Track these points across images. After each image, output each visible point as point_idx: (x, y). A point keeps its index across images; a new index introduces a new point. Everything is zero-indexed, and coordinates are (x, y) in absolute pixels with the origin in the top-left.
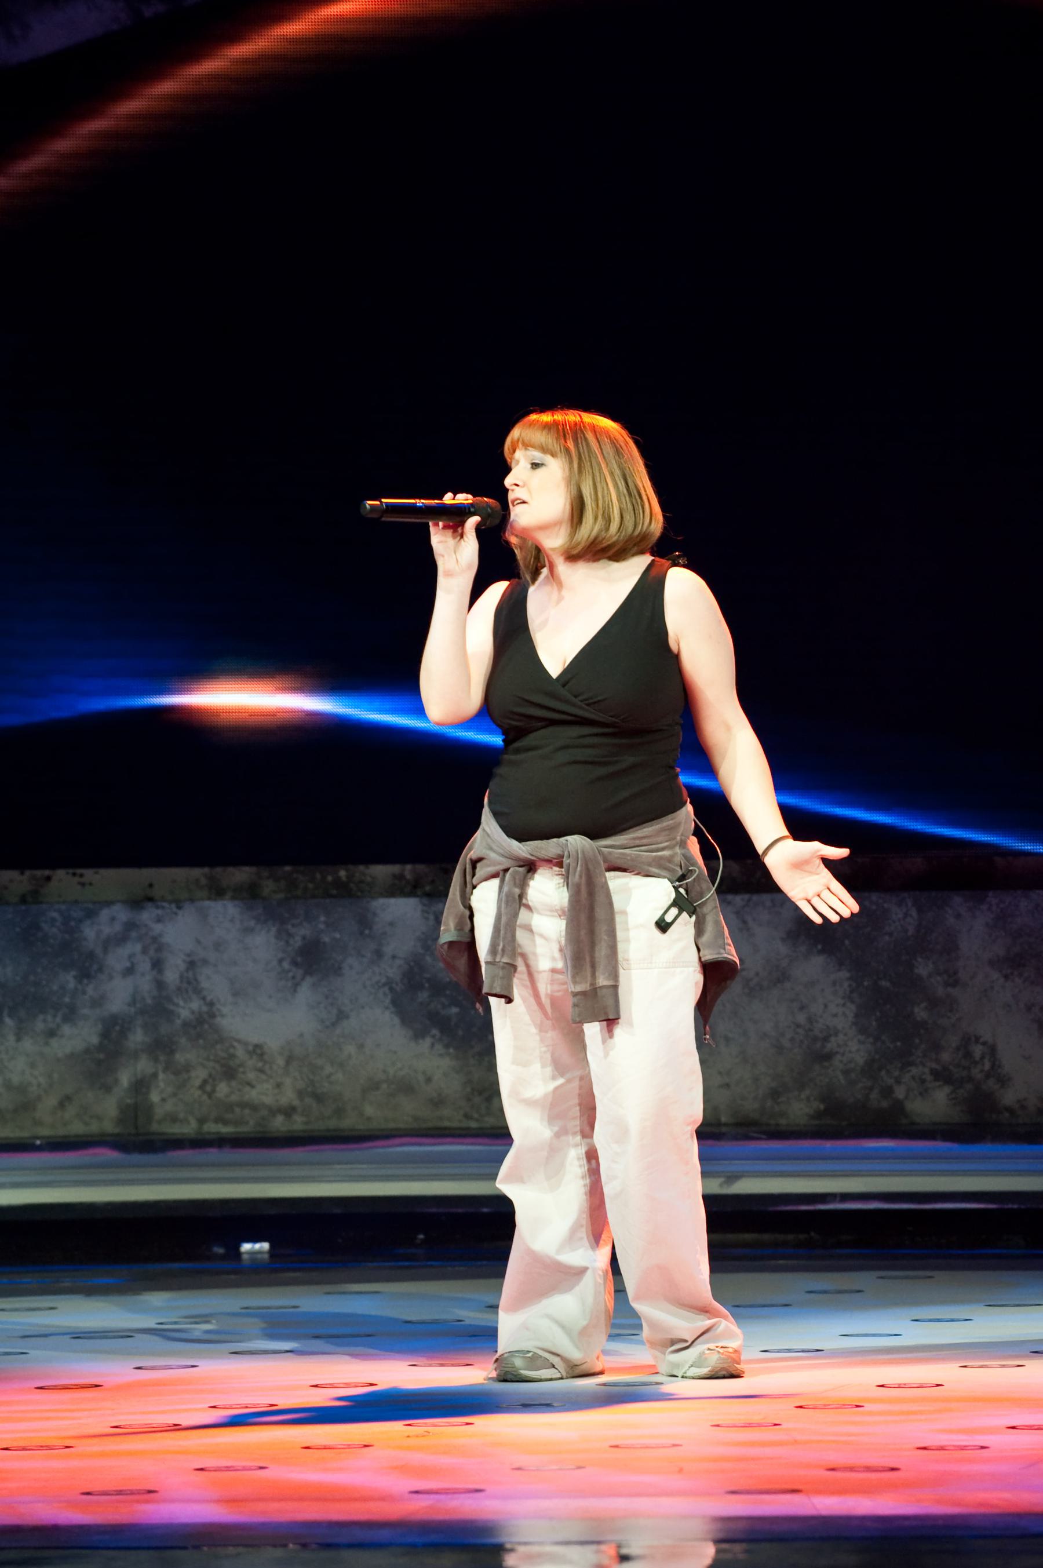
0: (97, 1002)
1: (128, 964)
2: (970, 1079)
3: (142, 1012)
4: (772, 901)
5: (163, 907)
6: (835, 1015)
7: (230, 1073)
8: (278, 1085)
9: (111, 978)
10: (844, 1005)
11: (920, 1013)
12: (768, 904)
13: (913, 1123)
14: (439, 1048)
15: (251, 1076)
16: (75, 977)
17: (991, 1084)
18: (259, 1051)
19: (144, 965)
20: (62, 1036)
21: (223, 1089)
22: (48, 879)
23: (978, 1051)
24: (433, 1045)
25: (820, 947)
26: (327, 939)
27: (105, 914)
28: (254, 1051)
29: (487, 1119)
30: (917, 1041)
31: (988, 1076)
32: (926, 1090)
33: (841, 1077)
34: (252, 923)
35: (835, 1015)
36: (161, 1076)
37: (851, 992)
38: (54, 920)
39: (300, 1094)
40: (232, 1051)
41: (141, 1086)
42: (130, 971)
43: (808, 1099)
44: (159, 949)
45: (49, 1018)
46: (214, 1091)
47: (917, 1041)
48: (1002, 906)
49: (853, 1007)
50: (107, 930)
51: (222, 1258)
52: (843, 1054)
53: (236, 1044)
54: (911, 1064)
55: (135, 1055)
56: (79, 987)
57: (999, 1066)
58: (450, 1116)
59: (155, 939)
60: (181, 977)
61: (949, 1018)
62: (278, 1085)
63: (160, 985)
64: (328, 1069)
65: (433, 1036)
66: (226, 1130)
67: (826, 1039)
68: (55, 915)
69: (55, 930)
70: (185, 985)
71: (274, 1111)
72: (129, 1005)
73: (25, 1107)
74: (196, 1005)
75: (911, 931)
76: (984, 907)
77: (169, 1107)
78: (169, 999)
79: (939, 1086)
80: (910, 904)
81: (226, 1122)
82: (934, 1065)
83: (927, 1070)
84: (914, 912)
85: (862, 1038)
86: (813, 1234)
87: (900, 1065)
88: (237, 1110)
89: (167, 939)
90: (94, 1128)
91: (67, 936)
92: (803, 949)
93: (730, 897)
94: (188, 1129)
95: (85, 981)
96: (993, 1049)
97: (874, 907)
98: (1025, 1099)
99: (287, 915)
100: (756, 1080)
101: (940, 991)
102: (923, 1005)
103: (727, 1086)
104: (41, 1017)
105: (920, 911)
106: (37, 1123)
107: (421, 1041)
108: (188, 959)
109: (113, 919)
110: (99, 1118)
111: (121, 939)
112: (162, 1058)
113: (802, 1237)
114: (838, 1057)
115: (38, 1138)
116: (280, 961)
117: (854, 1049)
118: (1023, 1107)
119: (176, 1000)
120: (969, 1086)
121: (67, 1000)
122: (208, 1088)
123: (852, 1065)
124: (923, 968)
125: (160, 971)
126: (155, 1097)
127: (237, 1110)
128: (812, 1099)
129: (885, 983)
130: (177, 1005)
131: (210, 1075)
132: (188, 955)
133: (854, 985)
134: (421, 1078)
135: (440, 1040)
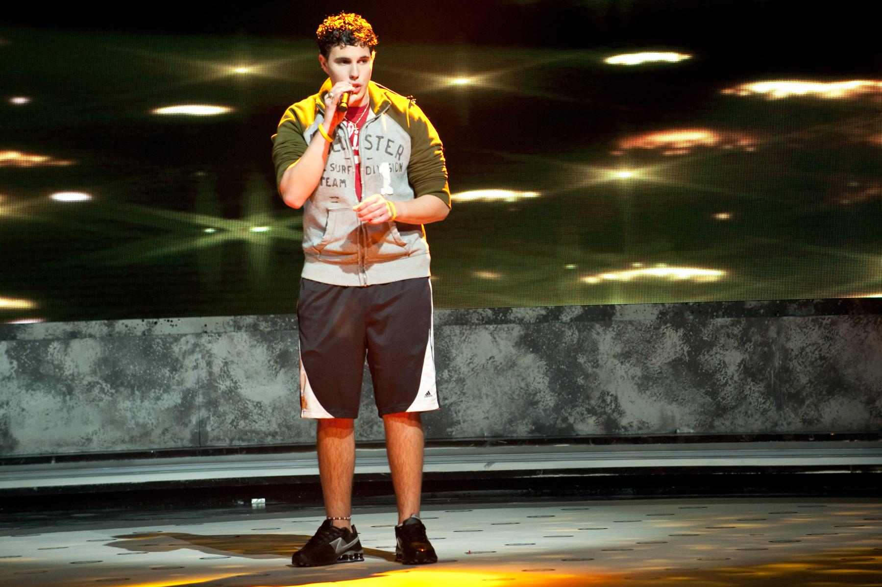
0: (180, 383)
1: (195, 364)
2: (605, 413)
3: (202, 387)
4: (508, 328)
5: (212, 336)
6: (539, 383)
7: (245, 416)
8: (269, 422)
9: (187, 371)
10: (543, 378)
11: (580, 381)
12: (506, 329)
13: (577, 435)
15: (256, 417)
16: (169, 371)
17: (616, 415)
18: (259, 405)
19: (203, 364)
20: (163, 400)
21: (242, 424)
22: (156, 323)
23: (609, 399)
25: (531, 349)
26: (292, 350)
27: (183, 339)
28: (257, 405)
29: (370, 436)
31: (614, 411)
32: (584, 418)
33: (543, 413)
34: (255, 343)
35: (539, 383)
36: (212, 418)
37: (547, 371)
38: (158, 343)
39: (279, 425)
40: (246, 405)
41: (202, 423)
42: (196, 367)
43: (527, 424)
44: (210, 357)
45: (157, 391)
46: (237, 425)
47: (579, 395)
48: (619, 328)
49: (548, 379)
50: (184, 348)
51: (244, 505)
52: (543, 402)
53: (248, 402)
54: (577, 406)
55: (199, 408)
56: (171, 375)
57: (619, 406)
59: (208, 352)
60: (221, 370)
62: (269, 422)
63: (211, 373)
64: (293, 413)
66: (244, 444)
67: (535, 394)
68: (160, 341)
70: (223, 373)
71: (267, 435)
72: (196, 384)
73: (146, 434)
75: (575, 340)
76: (611, 329)
77: (215, 433)
78: (215, 381)
79: (590, 417)
80: (575, 328)
81: (243, 440)
82: (587, 406)
83: (584, 409)
84: (577, 333)
85: (553, 394)
86: (530, 490)
88: (249, 434)
89: (213, 351)
90: (179, 444)
91: (165, 351)
92: (523, 351)
93: (487, 326)
94: (225, 444)
95: (174, 372)
96: (616, 398)
97: (557, 330)
98: (632, 422)
99: (272, 338)
100: (501, 415)
101: (590, 370)
102: (581, 377)
103: (487, 418)
104: (153, 390)
105: (579, 331)
106: (152, 442)
108: (224, 361)
109: (187, 342)
110: (182, 439)
111: (192, 352)
112: (212, 409)
113: (524, 491)
114: (541, 403)
115: (152, 449)
116: (269, 361)
117: (549, 399)
118: (631, 426)
119: (218, 381)
120: (605, 416)
121: (165, 382)
122: (235, 424)
123: (548, 407)
124: (581, 360)
125: (211, 367)
126: (209, 429)
127: (249, 434)
128: (528, 424)
130: (219, 384)
131: (235, 418)
132: (224, 359)
133: (548, 368)
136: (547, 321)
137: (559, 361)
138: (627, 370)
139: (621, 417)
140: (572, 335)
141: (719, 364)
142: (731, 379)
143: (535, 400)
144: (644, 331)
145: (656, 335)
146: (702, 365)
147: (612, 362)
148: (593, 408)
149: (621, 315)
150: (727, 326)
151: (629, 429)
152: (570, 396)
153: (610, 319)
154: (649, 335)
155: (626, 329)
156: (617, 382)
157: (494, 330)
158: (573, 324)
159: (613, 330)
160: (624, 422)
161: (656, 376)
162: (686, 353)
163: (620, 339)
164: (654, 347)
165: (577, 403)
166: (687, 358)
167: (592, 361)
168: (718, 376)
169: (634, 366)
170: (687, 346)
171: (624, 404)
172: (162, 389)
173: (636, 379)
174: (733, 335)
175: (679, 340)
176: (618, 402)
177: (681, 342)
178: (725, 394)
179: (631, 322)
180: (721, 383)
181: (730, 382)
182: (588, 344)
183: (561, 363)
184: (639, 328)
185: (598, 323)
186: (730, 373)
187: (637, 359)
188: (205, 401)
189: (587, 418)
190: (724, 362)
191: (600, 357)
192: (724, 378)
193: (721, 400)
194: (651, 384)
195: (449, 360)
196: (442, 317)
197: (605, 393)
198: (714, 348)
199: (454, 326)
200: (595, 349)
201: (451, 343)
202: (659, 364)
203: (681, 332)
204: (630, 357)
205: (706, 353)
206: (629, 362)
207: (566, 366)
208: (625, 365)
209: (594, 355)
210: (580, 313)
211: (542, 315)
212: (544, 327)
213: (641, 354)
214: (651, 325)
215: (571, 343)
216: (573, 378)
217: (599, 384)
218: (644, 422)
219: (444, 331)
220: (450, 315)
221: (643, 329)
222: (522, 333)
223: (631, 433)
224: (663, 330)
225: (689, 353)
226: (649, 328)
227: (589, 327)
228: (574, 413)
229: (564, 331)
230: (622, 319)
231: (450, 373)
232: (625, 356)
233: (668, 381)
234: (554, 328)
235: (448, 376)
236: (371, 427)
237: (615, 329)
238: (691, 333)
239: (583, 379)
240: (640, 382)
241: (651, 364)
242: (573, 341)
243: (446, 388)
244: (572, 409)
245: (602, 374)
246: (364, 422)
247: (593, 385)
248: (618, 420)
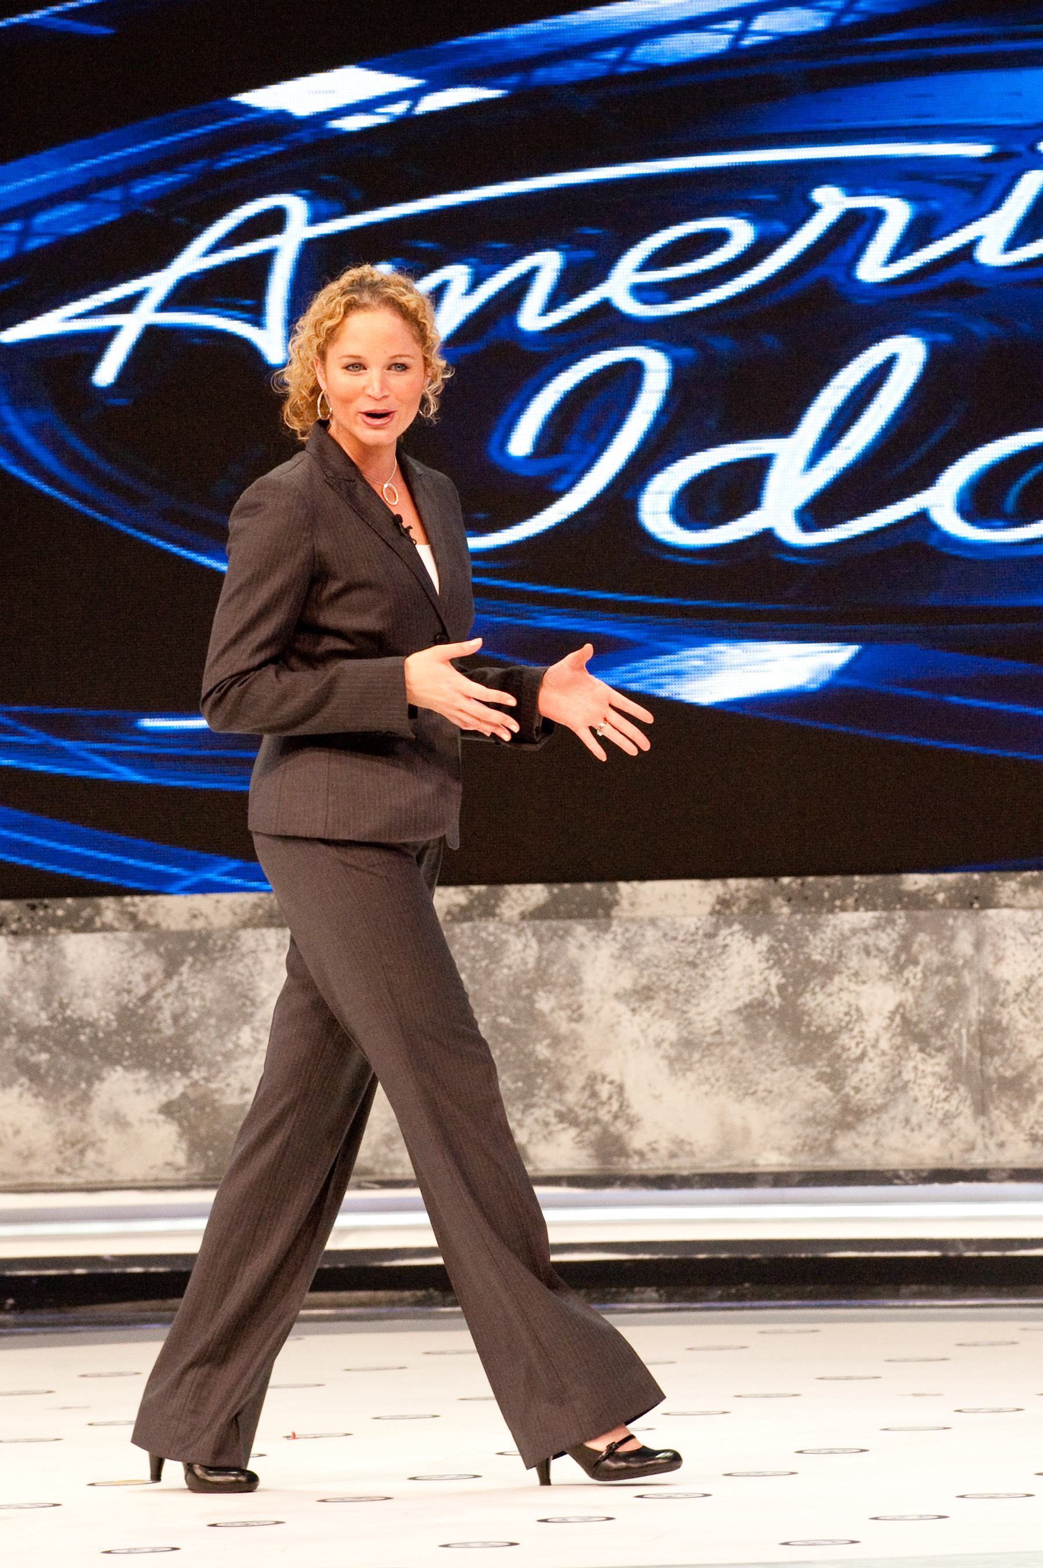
2: (597, 1121)
11: (542, 1050)
14: (28, 1097)
17: (620, 1127)
23: (604, 1090)
24: (21, 1096)
30: (539, 1081)
31: (616, 1117)
32: (550, 1133)
48: (628, 935)
54: (533, 1106)
57: (628, 1106)
58: (42, 1169)
61: (573, 1056)
65: (22, 1085)
75: (531, 963)
76: (609, 937)
79: (564, 1129)
80: (529, 934)
82: (558, 1106)
83: (551, 1112)
84: (534, 943)
87: (521, 1107)
96: (621, 1088)
97: (491, 939)
98: (656, 1142)
101: (564, 1027)
102: (546, 1042)
105: (540, 941)
107: (8, 1090)
118: (654, 1150)
120: (596, 1129)
124: (544, 1003)
129: (504, 1020)
134: (10, 1131)
135: (29, 1089)
136: (470, 919)
137: (496, 1007)
138: (644, 1026)
140: (524, 950)
141: (847, 1014)
142: (874, 1046)
144: (683, 941)
145: (710, 949)
146: (810, 1015)
147: (613, 1010)
148: (571, 1110)
149: (632, 904)
150: (865, 931)
151: (650, 1155)
152: (520, 1084)
153: (608, 915)
154: (692, 951)
155: (643, 935)
156: (624, 1053)
158: (525, 924)
159: (614, 939)
160: (637, 1141)
161: (709, 1039)
163: (630, 959)
164: (703, 976)
165: (535, 1100)
167: (569, 1006)
168: (845, 1039)
169: (661, 1017)
170: (777, 974)
171: (638, 1103)
173: (665, 1045)
174: (878, 949)
175: (760, 961)
176: (626, 1095)
177: (764, 965)
178: (861, 1080)
179: (653, 922)
180: (853, 1056)
181: (871, 1053)
182: (559, 970)
183: (501, 1011)
184: (672, 934)
185: (581, 924)
186: (870, 1035)
187: (667, 1002)
189: (558, 1132)
190: (858, 1010)
191: (583, 998)
192: (858, 1044)
193: (852, 1093)
194: (696, 1056)
195: (253, 1003)
196: (238, 910)
197: (595, 1078)
198: (837, 979)
199: (264, 931)
200: (573, 981)
201: (258, 967)
202: (715, 1013)
203: (764, 941)
204: (652, 998)
205: (817, 989)
206: (649, 1008)
207: (512, 1019)
208: (641, 1015)
209: (572, 994)
210: (542, 901)
211: (458, 905)
212: (462, 932)
213: (676, 991)
214: (697, 929)
215: (522, 967)
216: (527, 1044)
217: (584, 1057)
218: (682, 1141)
219: (242, 940)
220: (256, 906)
221: (680, 937)
223: (655, 1165)
224: (725, 939)
225: (781, 988)
226: (693, 935)
227: (561, 933)
228: (529, 1121)
229: (505, 943)
230: (632, 915)
231: (255, 1035)
233: (735, 1052)
234: (483, 934)
235: (251, 1041)
236: (82, 1152)
237: (619, 938)
238: (786, 946)
239: (549, 1046)
240: (673, 1053)
241: (699, 1014)
242: (526, 963)
243: (248, 1067)
244: (523, 1111)
245: (589, 1033)
246: (65, 1143)
247: (568, 1060)
248: (626, 1137)
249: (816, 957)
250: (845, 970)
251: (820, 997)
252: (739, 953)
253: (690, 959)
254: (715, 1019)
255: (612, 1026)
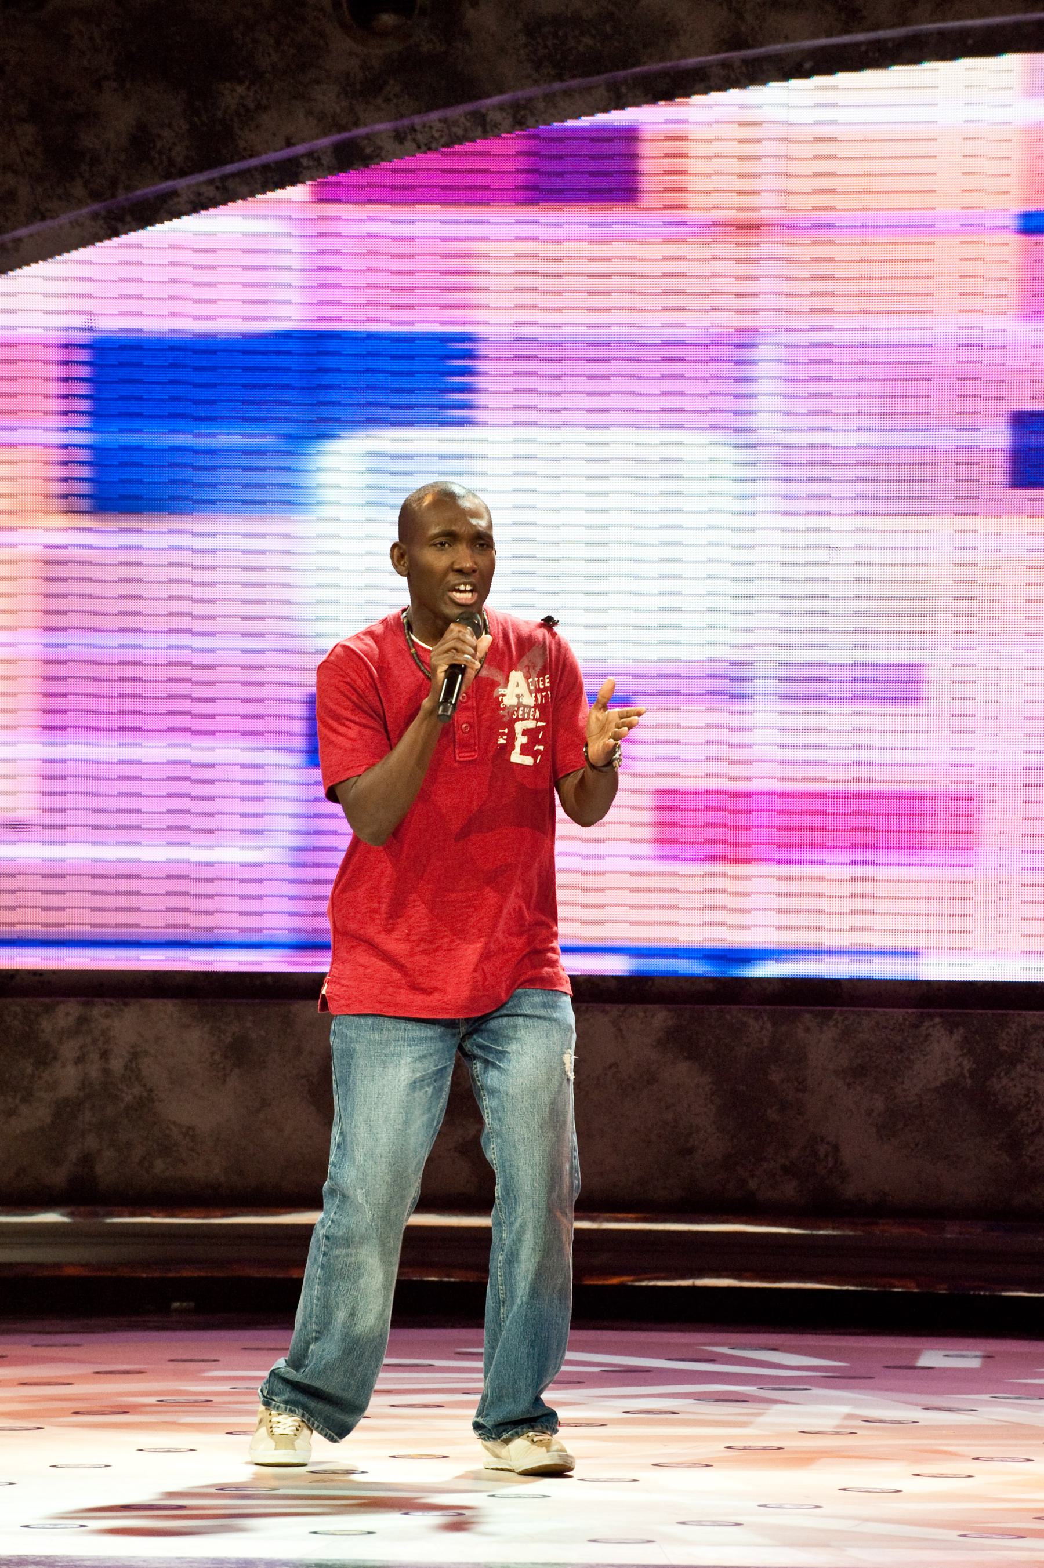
0: (53, 1086)
9: (64, 1066)
11: (772, 1115)
12: (641, 1014)
18: (191, 1133)
23: (822, 1150)
26: (254, 1036)
36: (107, 1153)
37: (713, 1095)
40: (168, 1132)
42: (80, 1060)
44: (107, 1041)
45: (10, 1100)
48: (847, 1022)
50: (62, 1023)
53: (172, 1127)
57: (841, 1164)
59: (104, 1032)
60: (126, 1068)
63: (106, 1072)
68: (18, 1009)
69: (16, 1023)
74: (137, 1091)
75: (766, 1040)
76: (831, 1023)
80: (766, 1019)
84: (769, 1026)
93: (608, 1007)
96: (836, 1148)
108: (132, 1050)
109: (68, 1014)
116: (213, 1054)
124: (776, 1076)
125: (107, 1060)
126: (99, 1169)
129: (742, 1087)
130: (122, 1091)
132: (132, 1047)
139: (842, 1182)
141: (1026, 1096)
143: (689, 1145)
146: (995, 1095)
154: (900, 1038)
157: (620, 1016)
159: (835, 1025)
162: (965, 1071)
164: (908, 1059)
166: (969, 1081)
168: (1023, 1116)
170: (969, 1061)
172: (19, 1096)
175: (955, 1049)
178: (1036, 1151)
188: (94, 1120)
190: (1036, 1092)
192: (1034, 1122)
193: (1028, 1161)
198: (1019, 1067)
203: (959, 1034)
205: (1002, 1074)
206: (862, 1083)
214: (905, 1020)
222: (670, 1023)
224: (927, 1029)
225: (971, 1072)
226: (900, 1025)
232: (857, 1073)
237: (839, 1025)
242: (762, 1043)
249: (1003, 1048)
250: (1027, 1060)
251: (1005, 1081)
252: (938, 1042)
253: (898, 1044)
254: (917, 1095)
255: (831, 1096)
